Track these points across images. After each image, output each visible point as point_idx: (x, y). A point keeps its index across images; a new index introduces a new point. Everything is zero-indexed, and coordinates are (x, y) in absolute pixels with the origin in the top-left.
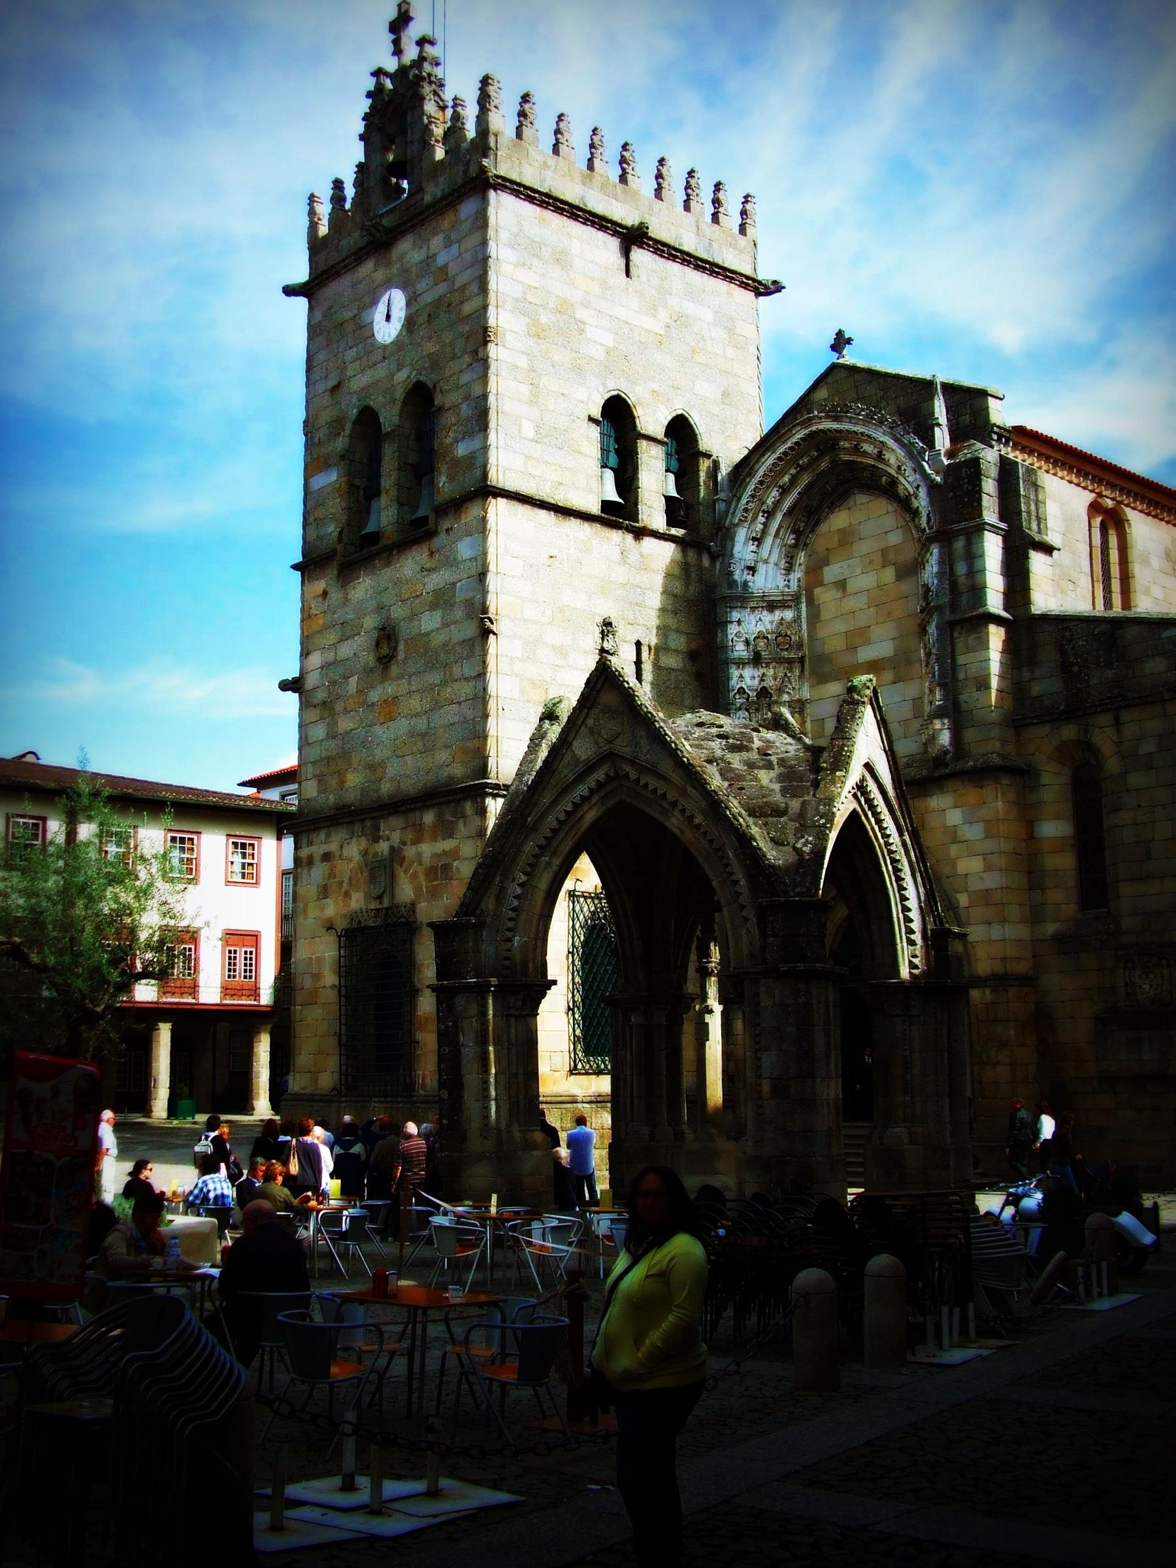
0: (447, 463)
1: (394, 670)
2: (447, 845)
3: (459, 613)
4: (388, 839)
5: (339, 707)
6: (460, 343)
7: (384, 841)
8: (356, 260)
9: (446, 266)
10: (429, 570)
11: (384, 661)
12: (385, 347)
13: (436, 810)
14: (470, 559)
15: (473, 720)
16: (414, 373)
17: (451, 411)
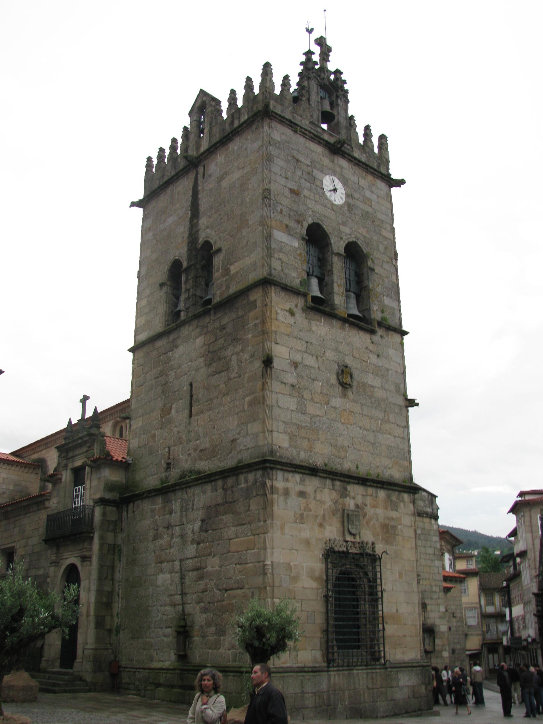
0: (378, 301)
1: (350, 393)
2: (394, 514)
3: (392, 388)
4: (354, 498)
5: (307, 395)
6: (382, 248)
7: (350, 498)
8: (311, 137)
9: (371, 200)
10: (371, 351)
11: (349, 387)
12: (332, 204)
13: (386, 492)
14: (396, 363)
15: (403, 449)
16: (353, 236)
17: (379, 276)
